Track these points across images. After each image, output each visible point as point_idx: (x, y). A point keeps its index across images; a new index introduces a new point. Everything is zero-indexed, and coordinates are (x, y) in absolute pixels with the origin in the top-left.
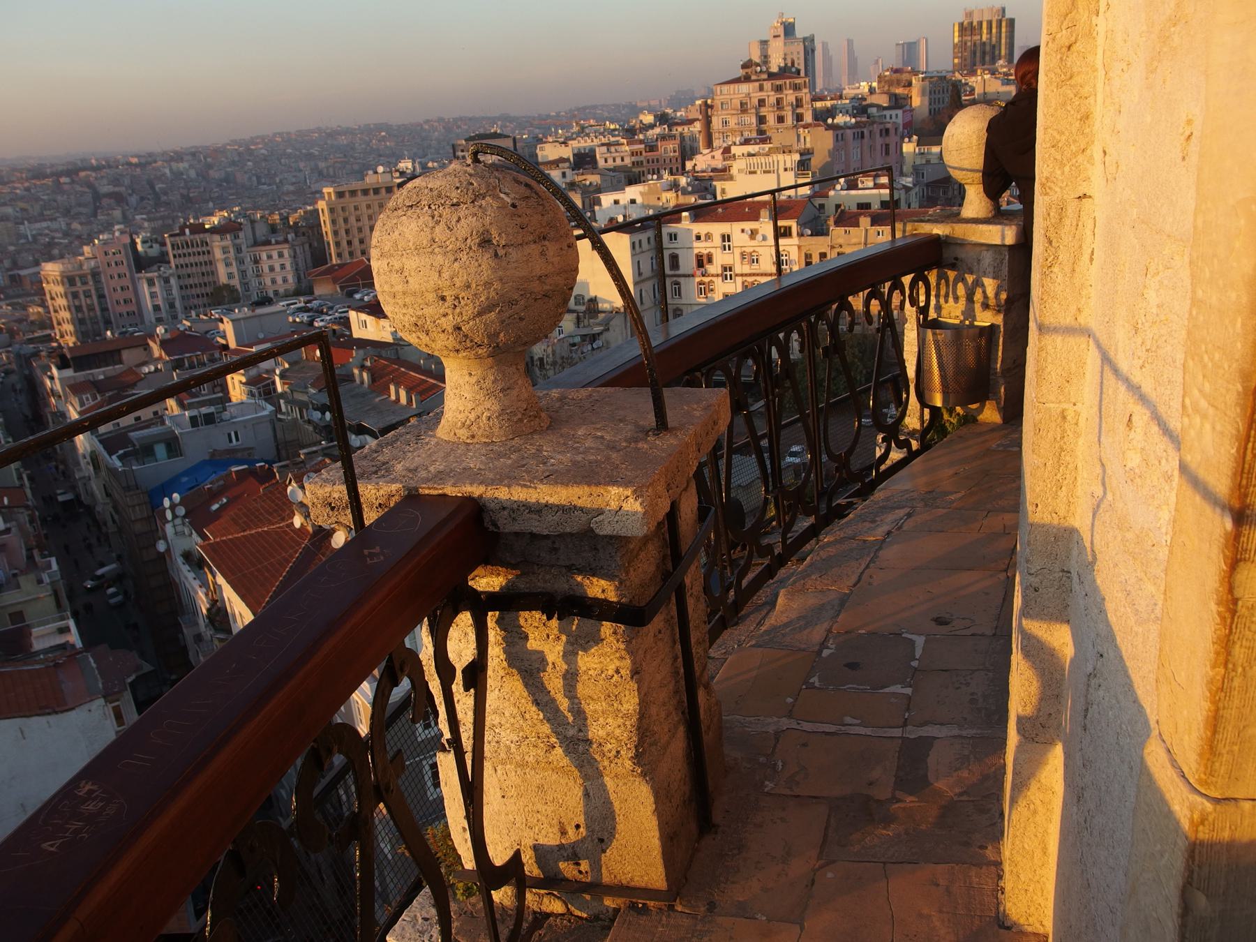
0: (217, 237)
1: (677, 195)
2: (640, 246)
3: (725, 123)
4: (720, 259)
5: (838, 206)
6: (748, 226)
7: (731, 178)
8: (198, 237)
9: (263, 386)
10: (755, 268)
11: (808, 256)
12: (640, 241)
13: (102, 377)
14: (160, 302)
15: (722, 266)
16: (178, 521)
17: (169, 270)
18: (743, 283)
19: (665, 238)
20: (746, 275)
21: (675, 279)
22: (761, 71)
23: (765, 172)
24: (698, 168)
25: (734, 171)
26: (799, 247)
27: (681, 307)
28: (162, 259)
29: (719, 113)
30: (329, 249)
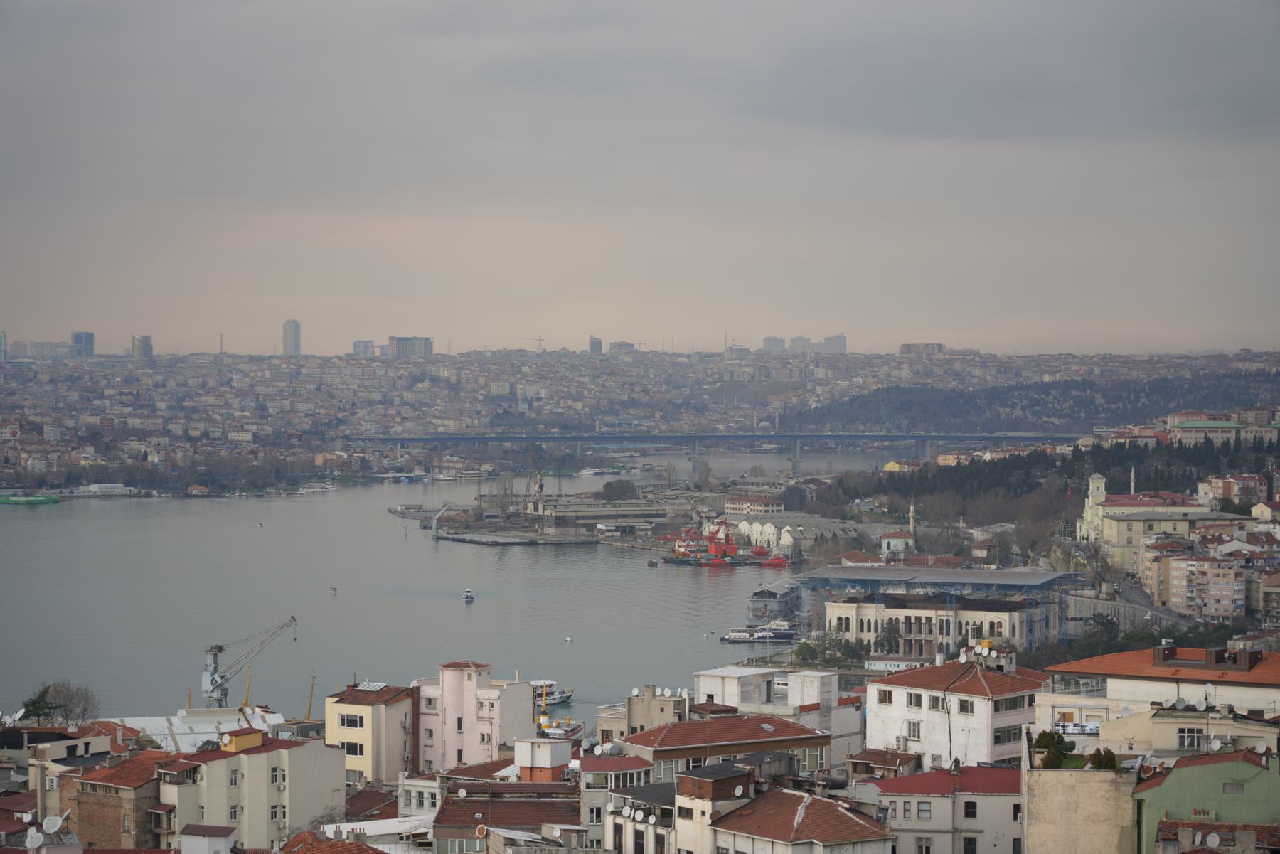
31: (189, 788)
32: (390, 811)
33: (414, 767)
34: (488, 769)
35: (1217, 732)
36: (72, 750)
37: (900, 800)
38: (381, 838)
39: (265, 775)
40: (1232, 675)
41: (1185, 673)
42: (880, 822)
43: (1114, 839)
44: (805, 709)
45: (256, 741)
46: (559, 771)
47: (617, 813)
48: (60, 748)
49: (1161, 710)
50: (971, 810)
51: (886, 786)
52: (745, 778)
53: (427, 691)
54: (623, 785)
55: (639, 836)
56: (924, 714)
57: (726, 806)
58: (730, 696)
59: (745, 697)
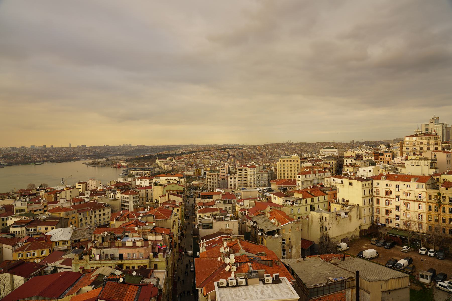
0: (249, 169)
1: (386, 170)
2: (366, 186)
3: (407, 149)
4: (395, 192)
5: (444, 179)
6: (407, 183)
7: (404, 166)
8: (244, 168)
9: (244, 212)
10: (408, 198)
11: (430, 196)
12: (366, 184)
13: (207, 202)
14: (233, 184)
15: (395, 195)
16: (204, 248)
17: (236, 176)
18: (403, 202)
19: (375, 185)
20: (405, 200)
21: (378, 198)
22: (422, 133)
23: (417, 165)
24: (395, 162)
25: (406, 165)
26: (426, 193)
27: (379, 207)
28: (235, 173)
29: (405, 146)
30: (278, 175)
31: (60, 194)
32: (84, 195)
33: (87, 190)
34: (95, 190)
35: (171, 182)
36: (46, 191)
37: (140, 190)
38: (83, 198)
39: (69, 192)
40: (172, 176)
41: (168, 176)
42: (138, 192)
43: (162, 192)
44: (129, 182)
45: (68, 189)
46: (103, 190)
47: (110, 193)
48: (44, 191)
49: (166, 180)
50: (147, 191)
51: (138, 189)
52: (124, 189)
53: (88, 182)
54: (110, 191)
55: (112, 196)
56: (142, 181)
57: (122, 192)
58: (121, 181)
59: (123, 181)
